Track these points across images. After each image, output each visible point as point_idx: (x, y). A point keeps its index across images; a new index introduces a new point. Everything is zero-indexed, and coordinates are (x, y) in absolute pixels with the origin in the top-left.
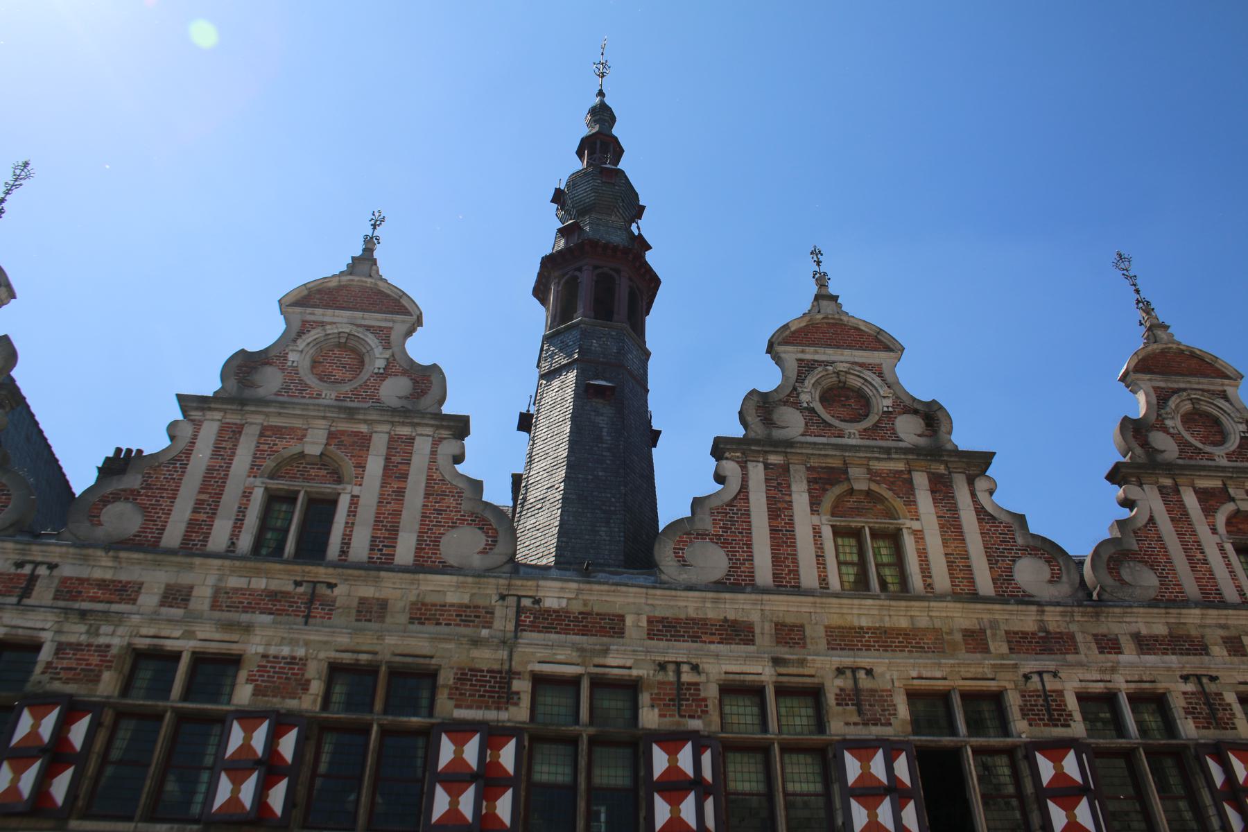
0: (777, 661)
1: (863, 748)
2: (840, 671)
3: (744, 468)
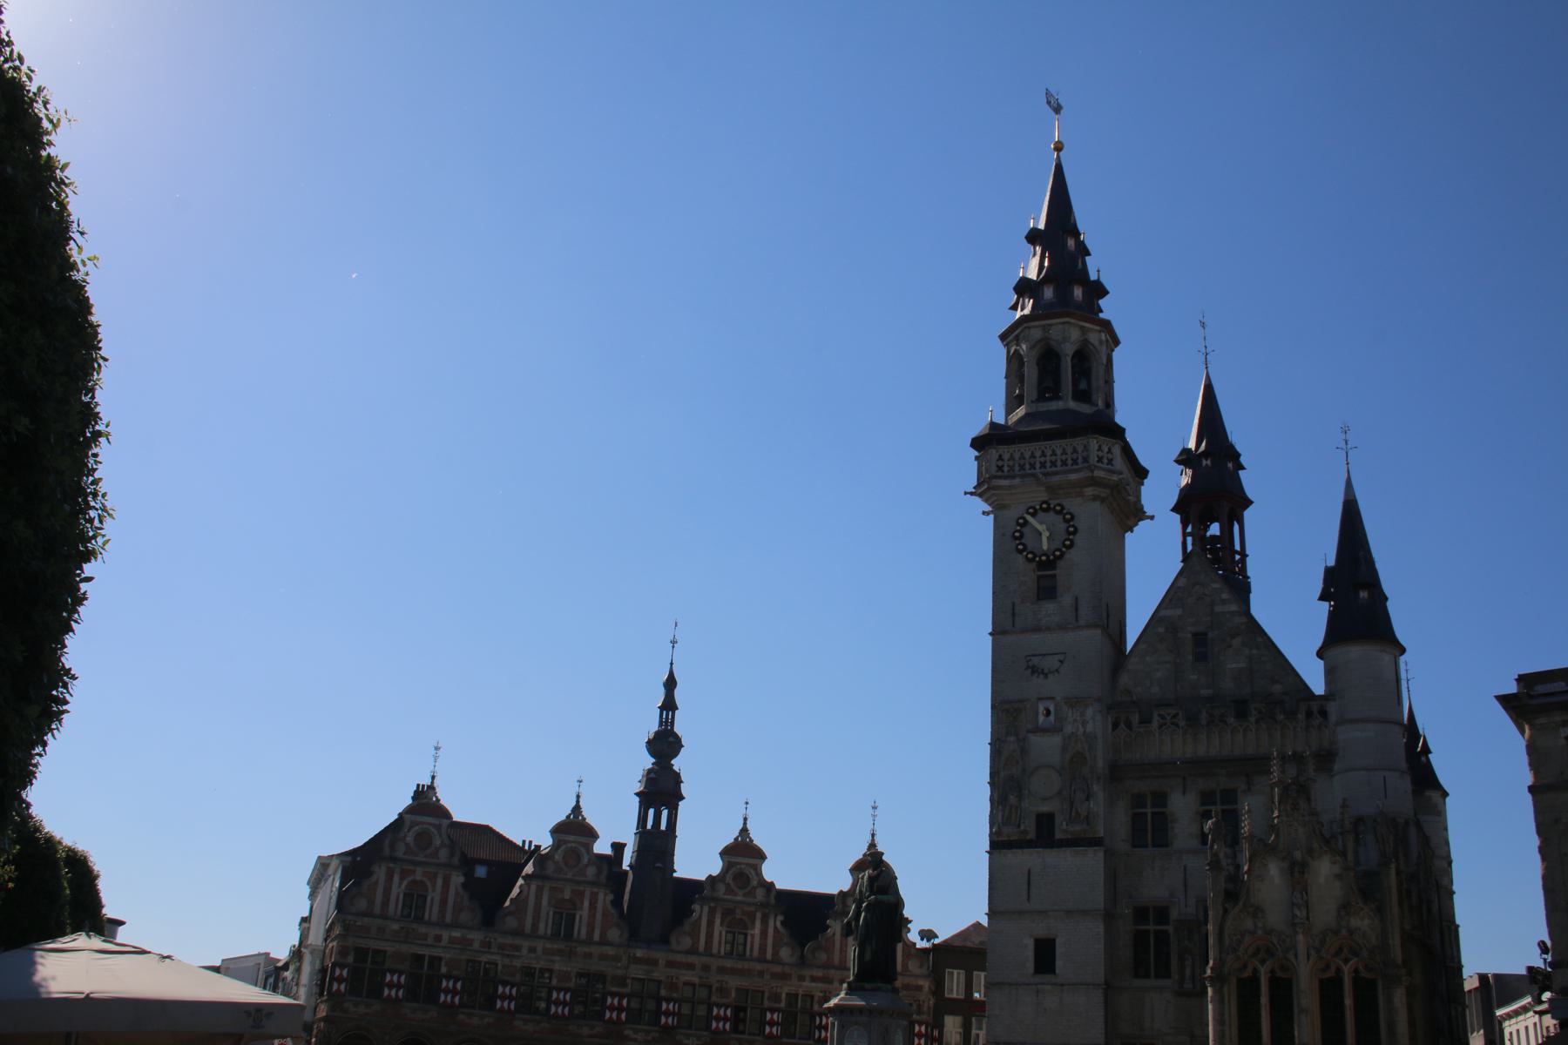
0: (701, 978)
1: (719, 1006)
2: (718, 981)
3: (702, 908)
